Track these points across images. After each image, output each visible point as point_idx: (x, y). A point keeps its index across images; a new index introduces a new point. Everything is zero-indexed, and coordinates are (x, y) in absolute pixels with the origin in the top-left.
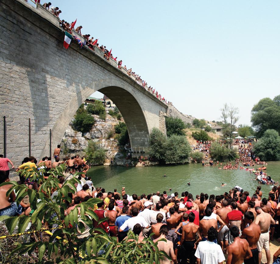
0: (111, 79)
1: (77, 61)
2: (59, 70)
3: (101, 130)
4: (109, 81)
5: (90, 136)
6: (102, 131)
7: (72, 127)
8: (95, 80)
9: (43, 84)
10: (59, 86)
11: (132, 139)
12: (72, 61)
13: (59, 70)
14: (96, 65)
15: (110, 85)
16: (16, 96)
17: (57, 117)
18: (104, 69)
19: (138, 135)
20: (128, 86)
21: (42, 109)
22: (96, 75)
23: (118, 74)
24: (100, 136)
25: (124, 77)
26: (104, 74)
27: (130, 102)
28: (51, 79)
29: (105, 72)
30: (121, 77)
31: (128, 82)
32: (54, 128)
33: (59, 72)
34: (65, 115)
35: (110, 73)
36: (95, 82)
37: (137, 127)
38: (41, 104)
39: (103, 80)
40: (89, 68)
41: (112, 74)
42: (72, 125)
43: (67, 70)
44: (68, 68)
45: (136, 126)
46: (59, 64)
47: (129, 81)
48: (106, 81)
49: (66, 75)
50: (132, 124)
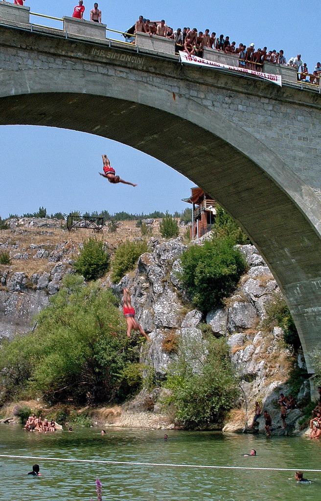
0: (19, 70)
3: (256, 296)
4: (8, 77)
5: (223, 323)
6: (260, 302)
7: (179, 296)
11: (300, 315)
15: (13, 92)
19: (314, 292)
20: (137, 81)
23: (57, 48)
24: (249, 323)
25: (94, 52)
27: (205, 148)
30: (80, 55)
31: (134, 68)
35: (10, 50)
37: (298, 257)
41: (21, 53)
42: (179, 289)
45: (294, 253)
47: (140, 62)
50: (276, 245)
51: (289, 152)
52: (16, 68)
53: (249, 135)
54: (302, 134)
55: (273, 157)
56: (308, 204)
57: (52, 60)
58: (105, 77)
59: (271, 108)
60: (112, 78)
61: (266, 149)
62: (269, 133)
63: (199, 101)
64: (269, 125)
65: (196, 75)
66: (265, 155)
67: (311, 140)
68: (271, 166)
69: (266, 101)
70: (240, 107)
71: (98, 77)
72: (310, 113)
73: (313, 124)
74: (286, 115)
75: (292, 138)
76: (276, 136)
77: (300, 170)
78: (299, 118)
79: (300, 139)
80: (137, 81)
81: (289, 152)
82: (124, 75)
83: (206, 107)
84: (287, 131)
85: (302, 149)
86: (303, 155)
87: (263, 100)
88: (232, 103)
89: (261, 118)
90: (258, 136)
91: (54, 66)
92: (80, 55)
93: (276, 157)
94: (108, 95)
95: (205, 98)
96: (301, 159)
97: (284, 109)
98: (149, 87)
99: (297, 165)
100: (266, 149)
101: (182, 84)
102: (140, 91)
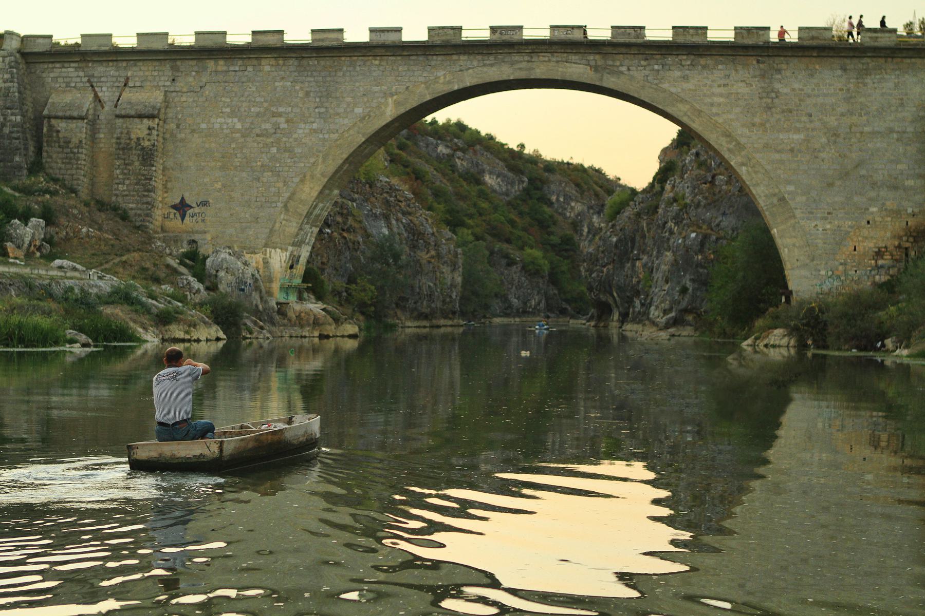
0: (461, 70)
1: (340, 74)
2: (301, 106)
8: (392, 95)
9: (274, 136)
10: (301, 131)
12: (328, 79)
13: (301, 106)
14: (399, 58)
15: (456, 88)
16: (236, 160)
17: (296, 180)
18: (430, 57)
21: (272, 171)
22: (397, 80)
26: (428, 68)
28: (286, 125)
29: (433, 63)
32: (290, 198)
33: (301, 108)
34: (312, 177)
36: (395, 97)
38: (270, 164)
39: (425, 83)
40: (374, 74)
43: (318, 100)
44: (319, 94)
46: (301, 94)
48: (438, 82)
49: (316, 108)
51: (708, 100)
52: (458, 69)
53: (665, 91)
54: (722, 82)
55: (688, 107)
56: (724, 144)
57: (486, 58)
58: (530, 64)
59: (689, 63)
60: (535, 63)
61: (683, 101)
62: (686, 86)
63: (615, 69)
64: (685, 78)
65: (610, 50)
66: (680, 106)
67: (732, 85)
68: (685, 114)
69: (685, 57)
70: (656, 67)
71: (524, 65)
72: (733, 61)
73: (736, 70)
74: (704, 67)
75: (711, 86)
76: (692, 87)
77: (717, 114)
78: (720, 67)
79: (719, 86)
80: (558, 62)
81: (708, 100)
82: (546, 59)
83: (622, 73)
84: (706, 81)
85: (721, 95)
86: (722, 100)
87: (680, 57)
88: (649, 65)
89: (678, 73)
90: (673, 90)
91: (488, 62)
92: (506, 51)
93: (692, 107)
94: (532, 77)
95: (621, 65)
96: (719, 104)
97: (703, 61)
98: (567, 64)
99: (714, 110)
100: (683, 101)
101: (597, 57)
102: (560, 69)
